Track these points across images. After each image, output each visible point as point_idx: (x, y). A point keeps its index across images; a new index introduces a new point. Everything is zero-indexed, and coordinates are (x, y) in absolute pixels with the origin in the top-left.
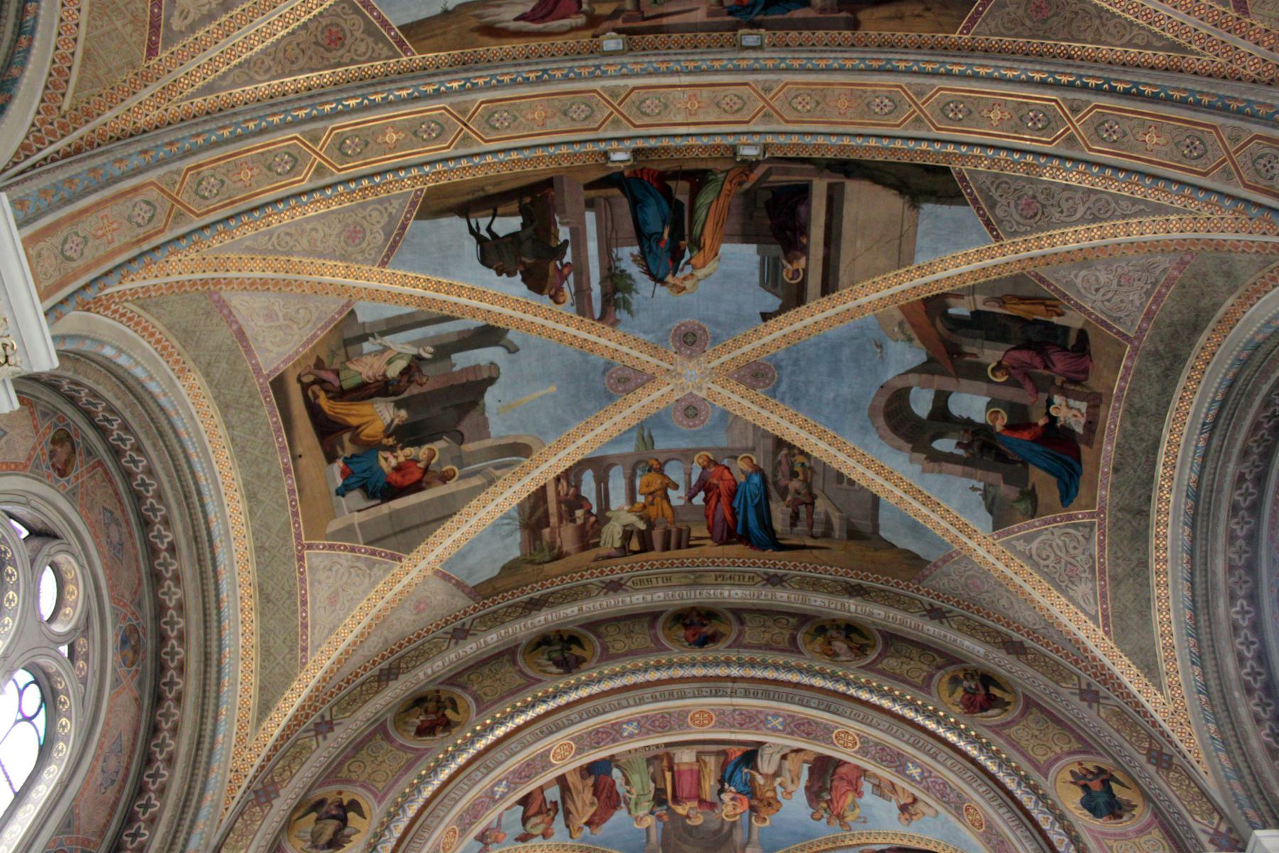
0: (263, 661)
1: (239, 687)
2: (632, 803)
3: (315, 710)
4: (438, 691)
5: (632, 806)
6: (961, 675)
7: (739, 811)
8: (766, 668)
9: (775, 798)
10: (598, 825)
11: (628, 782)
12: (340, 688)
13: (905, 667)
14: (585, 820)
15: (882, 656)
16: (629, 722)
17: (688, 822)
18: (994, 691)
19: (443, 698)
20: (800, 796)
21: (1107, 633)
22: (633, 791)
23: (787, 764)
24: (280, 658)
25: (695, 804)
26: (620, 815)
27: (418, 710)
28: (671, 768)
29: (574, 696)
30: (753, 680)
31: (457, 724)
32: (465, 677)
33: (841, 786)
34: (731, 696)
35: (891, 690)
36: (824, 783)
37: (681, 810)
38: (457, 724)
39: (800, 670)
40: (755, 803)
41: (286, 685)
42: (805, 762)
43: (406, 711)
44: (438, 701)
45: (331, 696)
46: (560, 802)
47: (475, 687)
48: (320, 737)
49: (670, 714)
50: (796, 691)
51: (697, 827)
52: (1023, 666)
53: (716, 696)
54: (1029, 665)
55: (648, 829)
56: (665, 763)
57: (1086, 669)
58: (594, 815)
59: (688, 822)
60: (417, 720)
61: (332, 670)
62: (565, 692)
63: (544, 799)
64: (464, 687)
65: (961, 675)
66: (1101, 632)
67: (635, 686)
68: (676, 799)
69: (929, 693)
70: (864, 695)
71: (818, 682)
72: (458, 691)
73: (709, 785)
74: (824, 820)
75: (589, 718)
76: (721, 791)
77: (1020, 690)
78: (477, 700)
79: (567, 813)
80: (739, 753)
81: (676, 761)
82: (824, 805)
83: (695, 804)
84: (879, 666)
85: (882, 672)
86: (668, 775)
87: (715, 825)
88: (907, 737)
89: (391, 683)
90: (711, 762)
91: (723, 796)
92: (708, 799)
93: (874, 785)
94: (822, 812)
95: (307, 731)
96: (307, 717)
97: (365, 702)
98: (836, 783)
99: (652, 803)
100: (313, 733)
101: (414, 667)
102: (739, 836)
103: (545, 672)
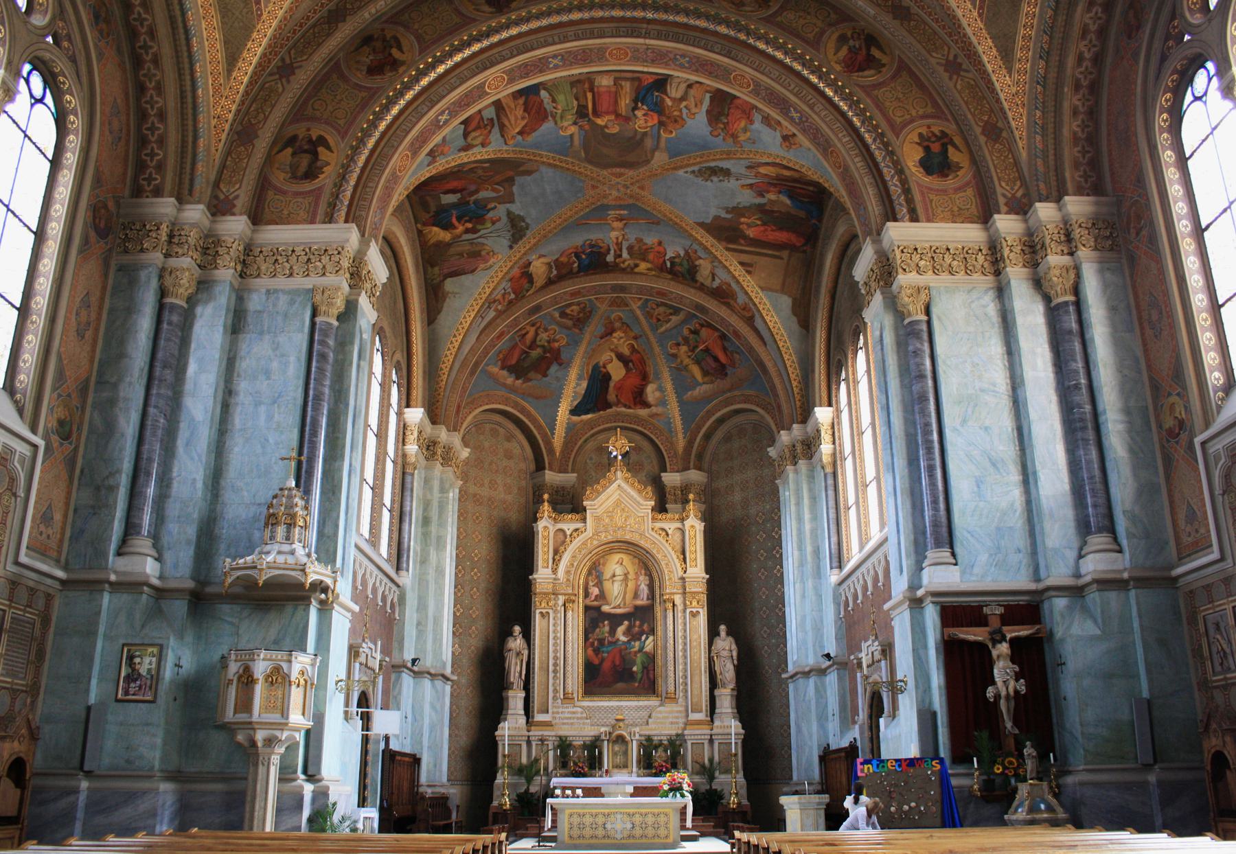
0: (223, 17)
1: (206, 43)
2: (558, 115)
3: (276, 55)
4: (383, 30)
5: (558, 118)
6: (849, 34)
7: (649, 124)
8: (678, 13)
10: (529, 134)
11: (554, 101)
12: (294, 32)
13: (802, 22)
14: (517, 130)
15: (783, 8)
16: (555, 57)
18: (875, 52)
19: (388, 37)
20: (702, 117)
21: (980, 15)
22: (559, 107)
23: (692, 92)
24: (237, 13)
25: (613, 117)
26: (548, 126)
27: (366, 49)
28: (591, 90)
29: (505, 35)
30: (665, 23)
31: (403, 63)
32: (407, 15)
34: (645, 38)
35: (785, 43)
37: (600, 122)
38: (403, 63)
39: (708, 17)
41: (247, 37)
43: (357, 49)
44: (384, 40)
45: (288, 40)
46: (495, 118)
47: (416, 27)
48: (284, 80)
49: (591, 50)
50: (702, 35)
51: (614, 135)
52: (905, 33)
53: (632, 36)
54: (910, 32)
55: (572, 136)
56: (587, 86)
57: (957, 42)
58: (525, 126)
59: (607, 131)
60: (367, 58)
61: (285, 19)
62: (497, 31)
64: (407, 27)
65: (849, 34)
66: (976, 14)
67: (561, 25)
68: (596, 113)
69: (818, 50)
70: (761, 46)
71: (723, 29)
72: (401, 29)
73: (625, 102)
74: (721, 137)
75: (519, 54)
76: (635, 108)
77: (897, 52)
78: (419, 38)
79: (502, 127)
82: (722, 126)
83: (613, 117)
84: (779, 19)
85: (781, 26)
86: (589, 96)
88: (793, 86)
89: (340, 25)
90: (627, 86)
91: (636, 112)
92: (624, 114)
93: (763, 117)
95: (271, 74)
96: (269, 62)
97: (319, 44)
98: (732, 111)
100: (277, 76)
101: (359, 8)
102: (649, 143)
103: (478, 10)
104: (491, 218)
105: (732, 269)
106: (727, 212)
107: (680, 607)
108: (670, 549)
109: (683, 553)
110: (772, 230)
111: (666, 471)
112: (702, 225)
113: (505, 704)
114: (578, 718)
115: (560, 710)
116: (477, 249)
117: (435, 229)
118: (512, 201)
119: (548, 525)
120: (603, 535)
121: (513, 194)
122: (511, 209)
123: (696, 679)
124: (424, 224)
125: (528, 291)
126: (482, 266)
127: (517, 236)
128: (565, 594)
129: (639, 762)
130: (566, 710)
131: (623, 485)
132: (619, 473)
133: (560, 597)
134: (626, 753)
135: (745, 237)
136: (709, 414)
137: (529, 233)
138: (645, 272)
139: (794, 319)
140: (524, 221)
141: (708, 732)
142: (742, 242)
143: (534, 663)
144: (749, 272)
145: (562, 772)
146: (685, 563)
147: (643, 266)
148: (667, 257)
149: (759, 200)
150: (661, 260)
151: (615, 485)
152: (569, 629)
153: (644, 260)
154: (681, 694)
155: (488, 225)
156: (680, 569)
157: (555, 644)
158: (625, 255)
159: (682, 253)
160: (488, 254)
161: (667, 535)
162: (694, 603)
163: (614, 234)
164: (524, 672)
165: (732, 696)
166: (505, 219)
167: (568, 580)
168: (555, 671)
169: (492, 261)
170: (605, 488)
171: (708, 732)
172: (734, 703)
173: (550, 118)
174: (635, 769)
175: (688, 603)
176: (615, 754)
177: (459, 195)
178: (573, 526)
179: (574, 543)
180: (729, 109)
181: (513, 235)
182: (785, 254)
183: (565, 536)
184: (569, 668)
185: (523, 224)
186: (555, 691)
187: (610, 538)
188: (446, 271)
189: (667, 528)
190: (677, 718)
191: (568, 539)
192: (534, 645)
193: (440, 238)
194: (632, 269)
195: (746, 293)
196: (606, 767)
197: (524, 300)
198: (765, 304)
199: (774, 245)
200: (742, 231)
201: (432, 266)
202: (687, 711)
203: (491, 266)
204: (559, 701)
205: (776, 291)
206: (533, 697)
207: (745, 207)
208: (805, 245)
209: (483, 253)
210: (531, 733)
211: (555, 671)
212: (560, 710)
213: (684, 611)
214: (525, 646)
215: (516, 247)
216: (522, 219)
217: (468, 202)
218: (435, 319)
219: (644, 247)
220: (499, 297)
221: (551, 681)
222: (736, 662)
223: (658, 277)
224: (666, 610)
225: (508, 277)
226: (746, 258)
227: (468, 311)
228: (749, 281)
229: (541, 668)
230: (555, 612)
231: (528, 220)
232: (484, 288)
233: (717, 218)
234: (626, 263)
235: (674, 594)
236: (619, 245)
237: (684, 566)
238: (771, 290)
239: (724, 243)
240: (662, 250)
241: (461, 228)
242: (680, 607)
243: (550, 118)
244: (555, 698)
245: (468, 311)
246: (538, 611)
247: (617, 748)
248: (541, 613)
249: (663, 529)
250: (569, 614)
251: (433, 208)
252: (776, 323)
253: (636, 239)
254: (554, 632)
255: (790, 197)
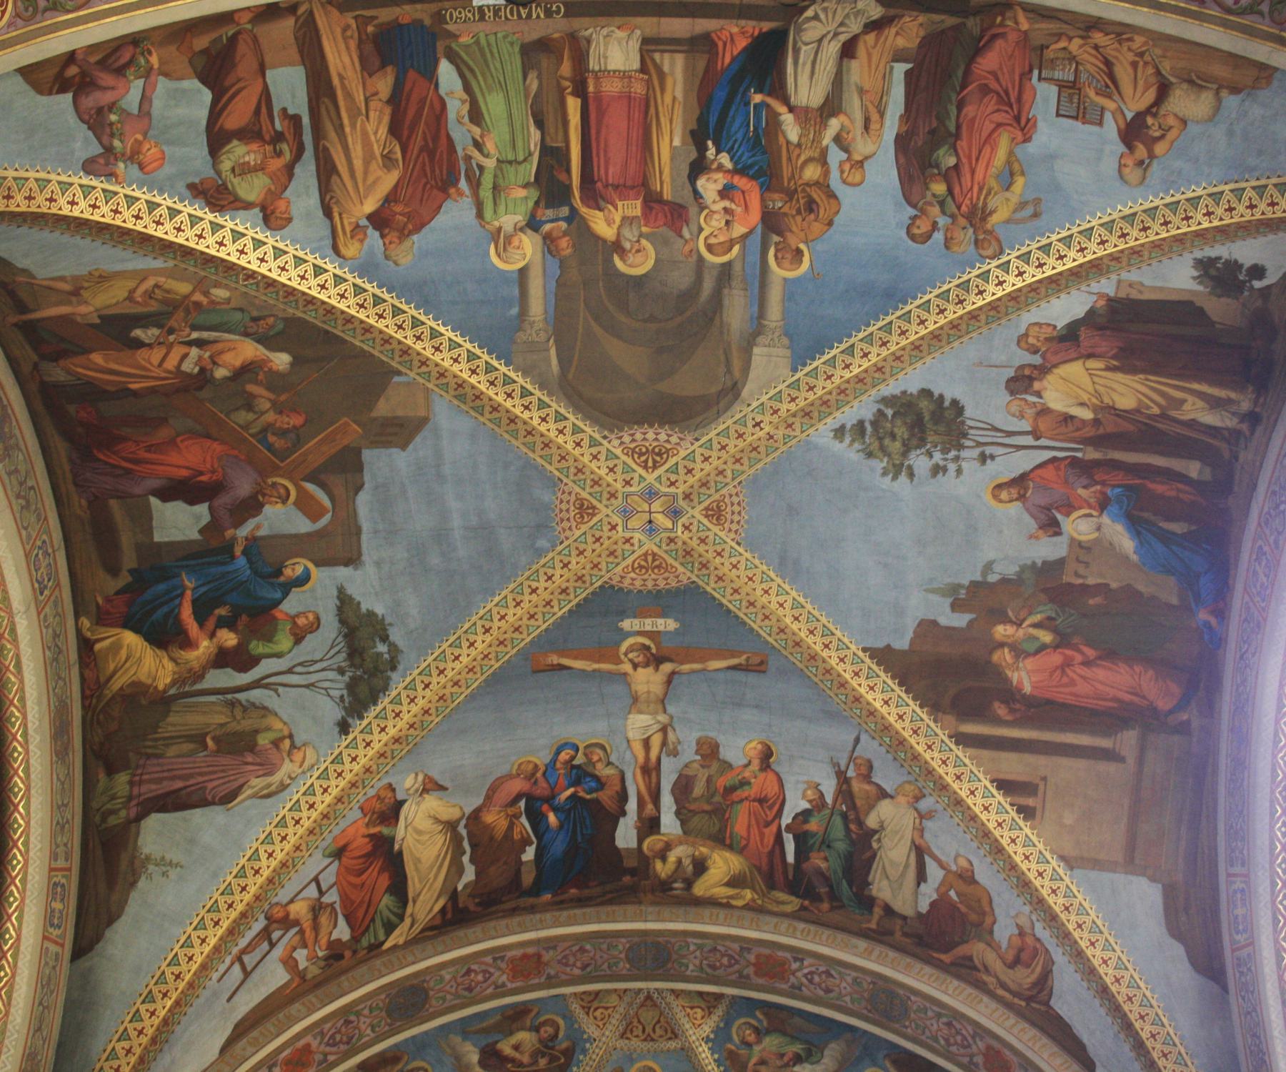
2: (487, 181)
5: (486, 193)
7: (739, 230)
9: (822, 184)
10: (404, 234)
11: (476, 115)
14: (370, 206)
17: (616, 259)
22: (490, 146)
23: (857, 71)
25: (634, 207)
33: (981, 112)
36: (942, 120)
37: (602, 224)
40: (777, 202)
42: (899, 57)
46: (306, 120)
51: (639, 281)
55: (523, 272)
56: (566, 69)
58: (391, 198)
59: (616, 259)
63: (266, 96)
74: (938, 237)
76: (698, 168)
79: (326, 171)
80: (742, 43)
81: (593, 64)
82: (939, 188)
83: (634, 207)
86: (573, 105)
87: (680, 279)
90: (675, 66)
91: (701, 183)
92: (667, 195)
93: (1062, 85)
94: (935, 210)
98: (969, 110)
99: (534, 194)
102: (736, 312)
104: (293, 619)
105: (976, 804)
106: (956, 606)
110: (1087, 663)
112: (883, 656)
116: (246, 724)
117: (130, 638)
118: (352, 559)
121: (359, 531)
122: (351, 590)
124: (103, 619)
125: (390, 928)
126: (257, 783)
127: (363, 690)
135: (1010, 695)
137: (398, 685)
138: (722, 892)
139: (1178, 950)
140: (385, 639)
142: (1001, 710)
144: (1027, 812)
147: (722, 864)
148: (786, 819)
149: (1048, 549)
150: (774, 828)
153: (721, 840)
155: (284, 641)
158: (669, 822)
159: (829, 788)
160: (276, 743)
163: (639, 724)
166: (331, 627)
169: (287, 768)
173: (463, 184)
177: (202, 509)
180: (960, 106)
181: (352, 687)
182: (1128, 740)
185: (382, 648)
188: (150, 790)
193: (143, 676)
194: (689, 884)
195: (1024, 885)
197: (378, 963)
198: (1082, 911)
199: (1093, 713)
200: (998, 673)
201: (111, 771)
203: (283, 787)
205: (1110, 866)
207: (1005, 581)
208: (1179, 707)
209: (263, 740)
215: (358, 726)
216: (379, 628)
217: (227, 550)
218: (98, 938)
219: (723, 781)
220: (299, 909)
223: (761, 910)
225: (327, 841)
226: (1015, 765)
227: (201, 925)
228: (1028, 843)
231: (396, 635)
232: (255, 856)
233: (927, 628)
234: (672, 857)
236: (650, 770)
238: (1096, 864)
239: (950, 719)
240: (771, 789)
241: (205, 647)
243: (463, 184)
245: (201, 925)
251: (129, 560)
252: (1120, 966)
253: (700, 743)
255: (1135, 523)
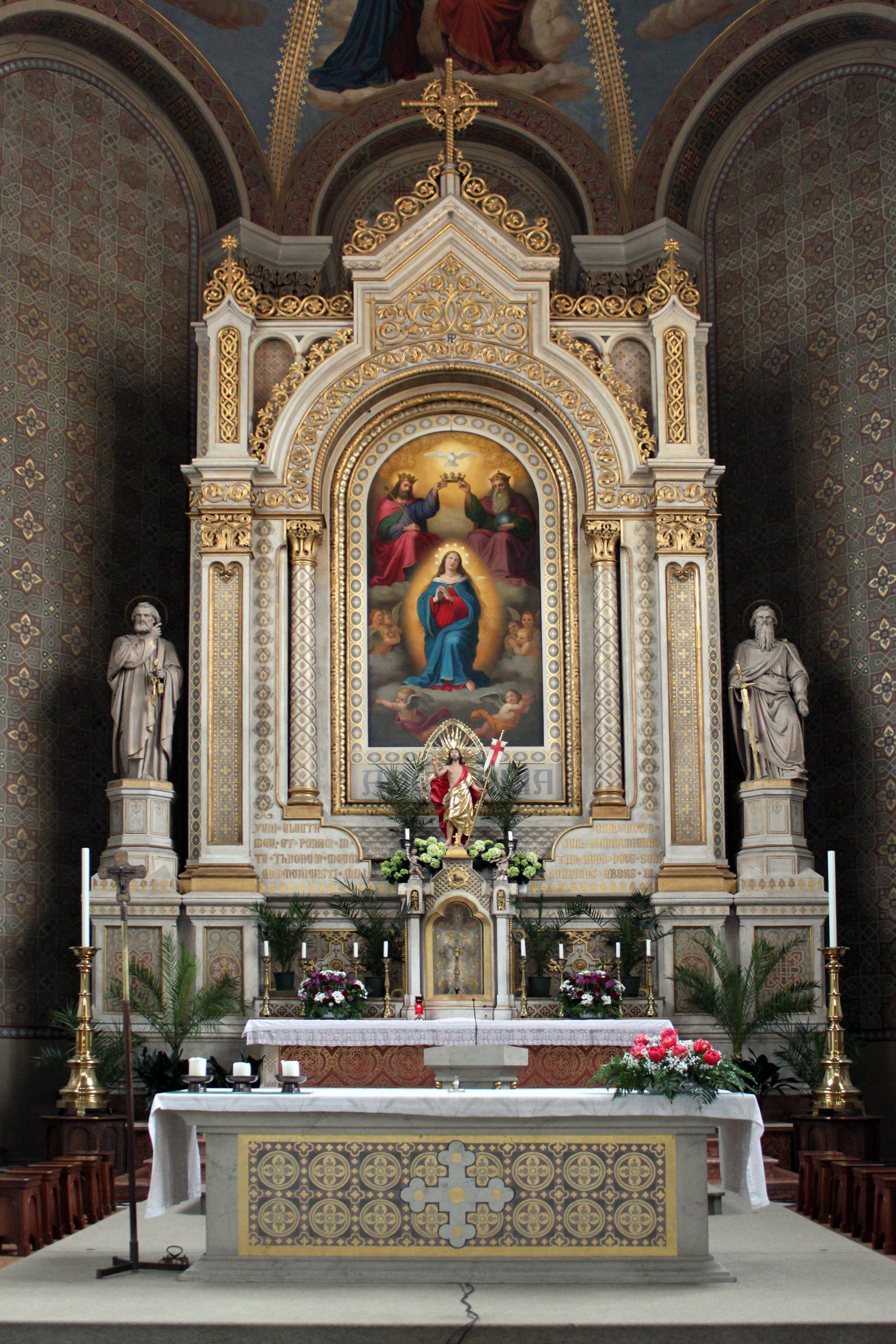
107: (635, 554)
108: (606, 392)
109: (646, 403)
111: (584, 232)
113: (114, 820)
114: (331, 859)
115: (279, 836)
119: (236, 322)
120: (401, 356)
123: (687, 751)
128: (289, 517)
129: (515, 978)
130: (297, 836)
131: (464, 211)
132: (451, 181)
133: (275, 524)
134: (475, 953)
136: (714, 64)
141: (725, 896)
143: (197, 707)
145: (279, 1003)
146: (653, 430)
151: (438, 212)
152: (304, 614)
154: (642, 795)
156: (635, 448)
157: (259, 656)
161: (598, 354)
162: (682, 542)
164: (168, 731)
165: (793, 798)
167: (298, 476)
168: (261, 729)
170: (403, 223)
171: (725, 896)
172: (799, 819)
174: (503, 997)
175: (661, 540)
176: (442, 955)
178: (311, 330)
179: (314, 374)
183: (290, 356)
184: (304, 722)
186: (263, 783)
187: (425, 362)
189: (595, 335)
190: (630, 859)
191: (299, 362)
192: (197, 655)
196: (415, 991)
202: (657, 841)
204: (276, 811)
206: (198, 800)
210: (188, 898)
211: (261, 729)
212: (279, 836)
213: (649, 566)
214: (174, 660)
221: (249, 757)
222: (804, 709)
224: (593, 564)
229: (218, 719)
230: (259, 565)
235: (617, 517)
237: (648, 440)
242: (635, 554)
244: (261, 803)
246: (207, 561)
247: (446, 939)
248: (217, 565)
249: (583, 340)
250: (304, 575)
254: (257, 620)
